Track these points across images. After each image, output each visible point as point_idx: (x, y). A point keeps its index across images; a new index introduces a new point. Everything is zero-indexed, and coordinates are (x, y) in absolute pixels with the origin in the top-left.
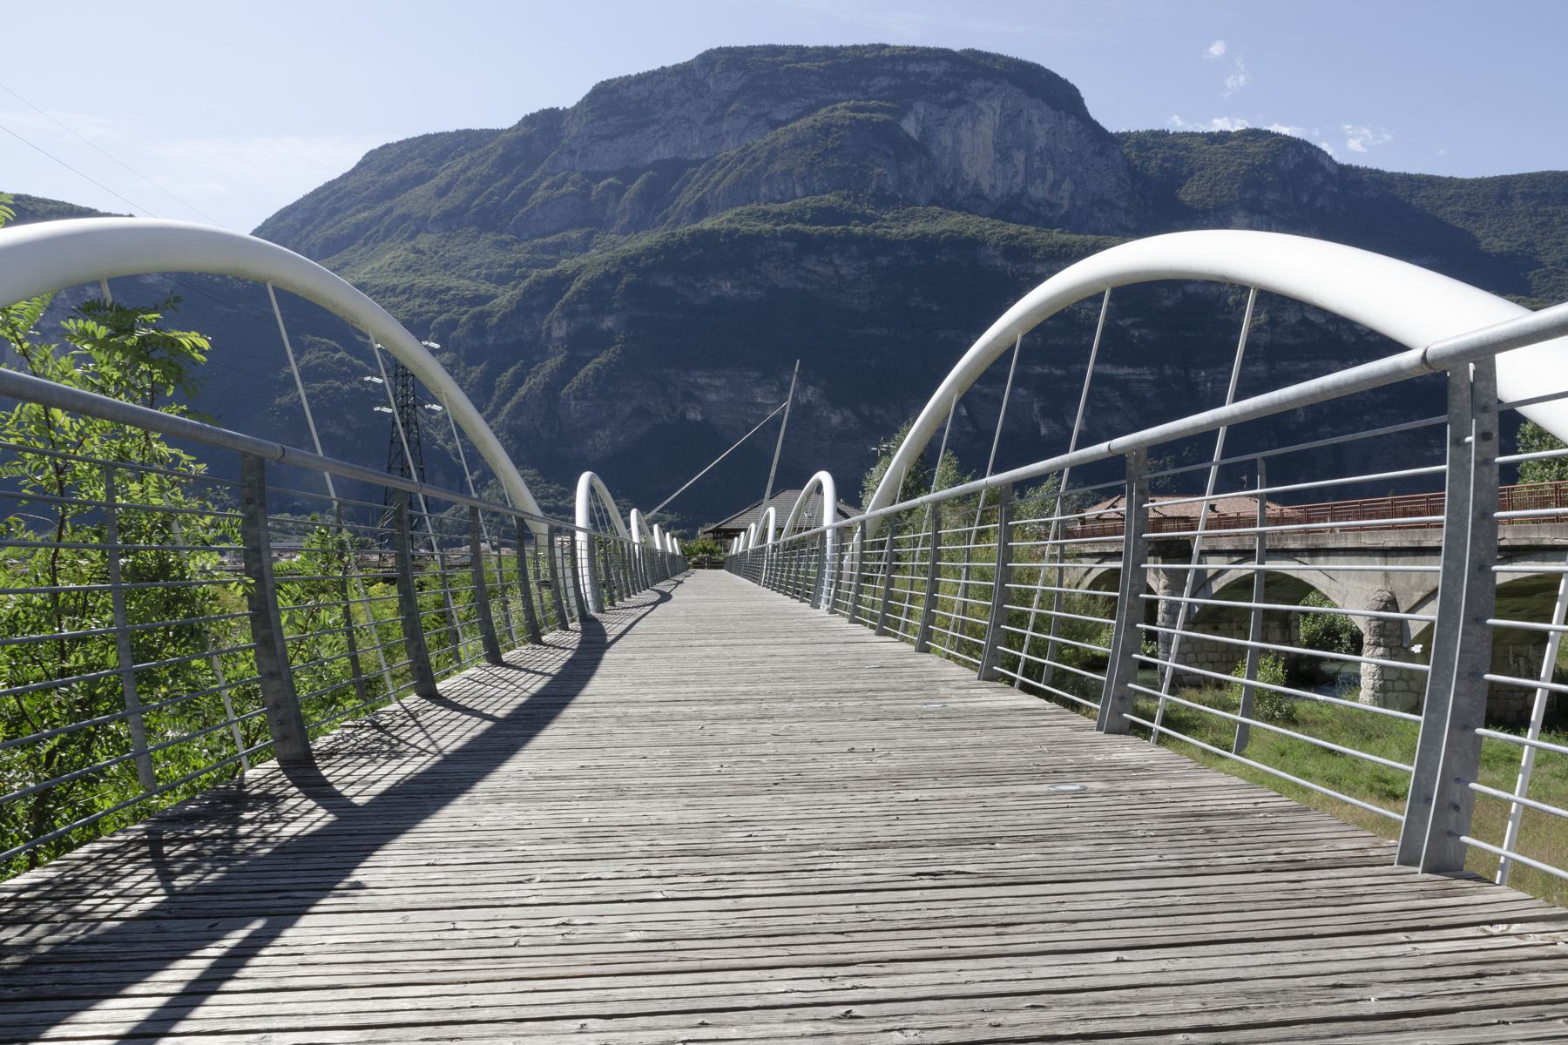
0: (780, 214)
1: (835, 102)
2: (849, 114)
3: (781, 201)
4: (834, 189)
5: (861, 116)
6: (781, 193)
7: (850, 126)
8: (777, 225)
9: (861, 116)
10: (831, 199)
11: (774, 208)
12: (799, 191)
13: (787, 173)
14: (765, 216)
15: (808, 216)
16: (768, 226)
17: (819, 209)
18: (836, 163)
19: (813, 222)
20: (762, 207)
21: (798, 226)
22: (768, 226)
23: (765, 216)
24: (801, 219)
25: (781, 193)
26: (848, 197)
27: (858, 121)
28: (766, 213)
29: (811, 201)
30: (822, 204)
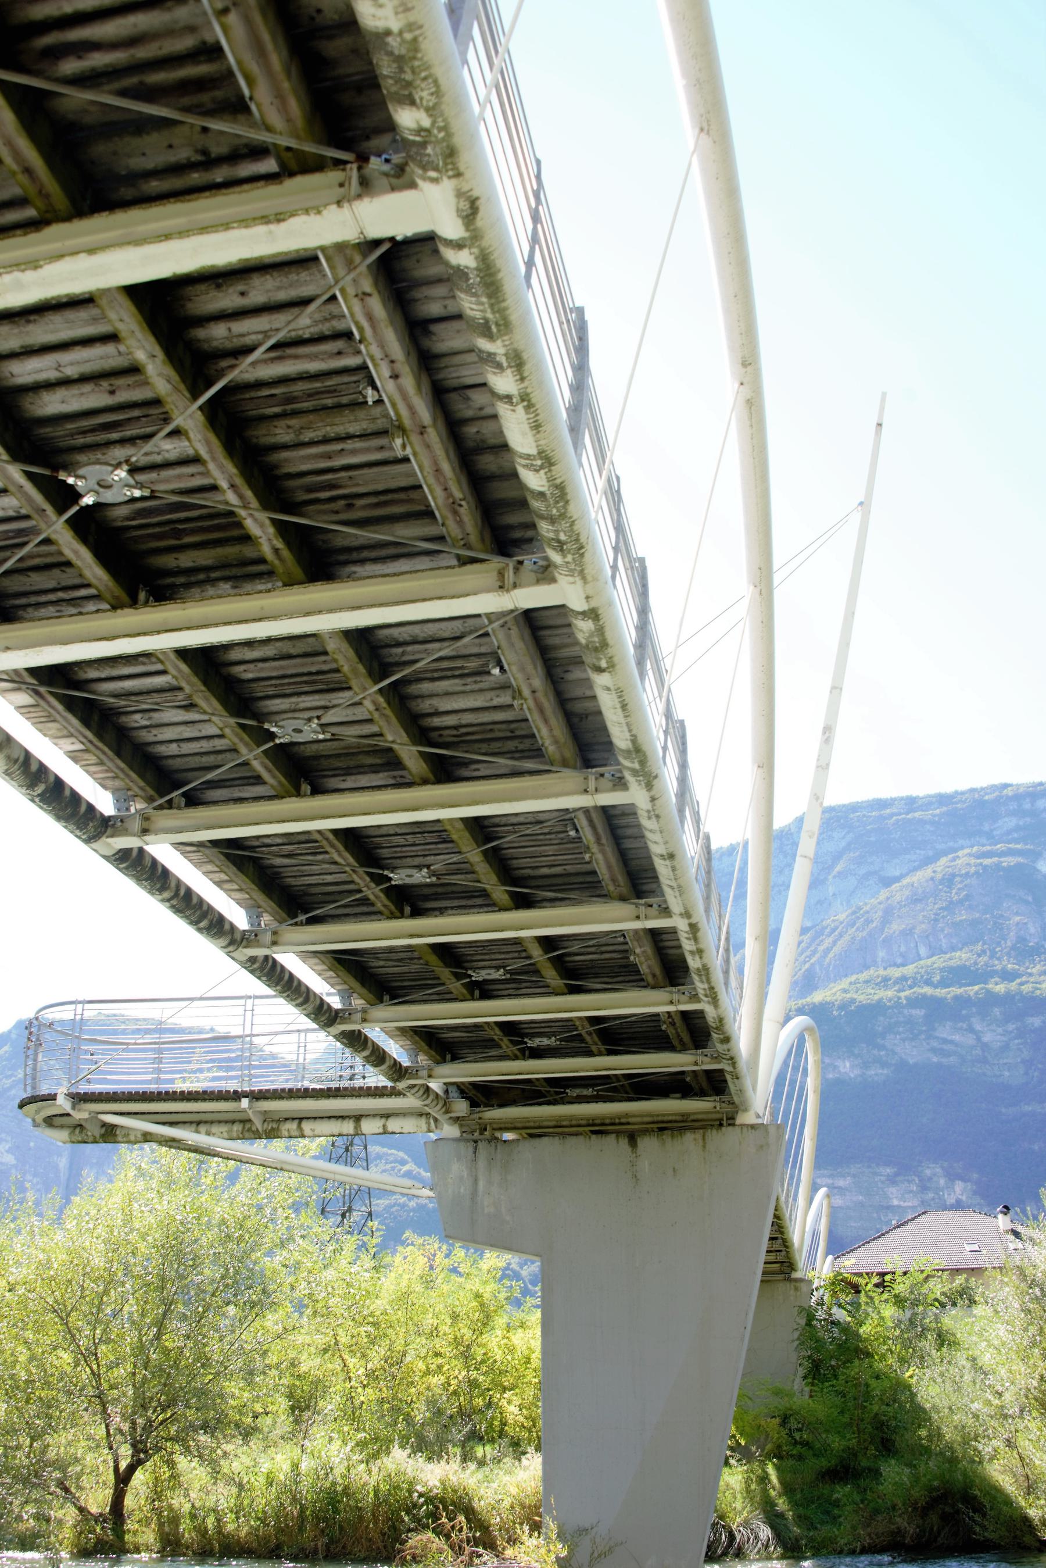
0: (904, 978)
1: (956, 850)
2: (973, 861)
3: (903, 965)
4: (965, 944)
5: (987, 862)
6: (902, 955)
7: (976, 873)
8: (899, 991)
9: (987, 862)
10: (962, 957)
11: (896, 973)
12: (923, 951)
13: (907, 933)
14: (885, 982)
15: (937, 978)
16: (890, 993)
17: (951, 970)
18: (962, 915)
19: (943, 983)
20: (881, 972)
21: (928, 990)
22: (890, 993)
23: (885, 982)
24: (928, 983)
25: (902, 955)
26: (984, 952)
27: (985, 868)
28: (886, 979)
29: (938, 961)
30: (952, 963)
